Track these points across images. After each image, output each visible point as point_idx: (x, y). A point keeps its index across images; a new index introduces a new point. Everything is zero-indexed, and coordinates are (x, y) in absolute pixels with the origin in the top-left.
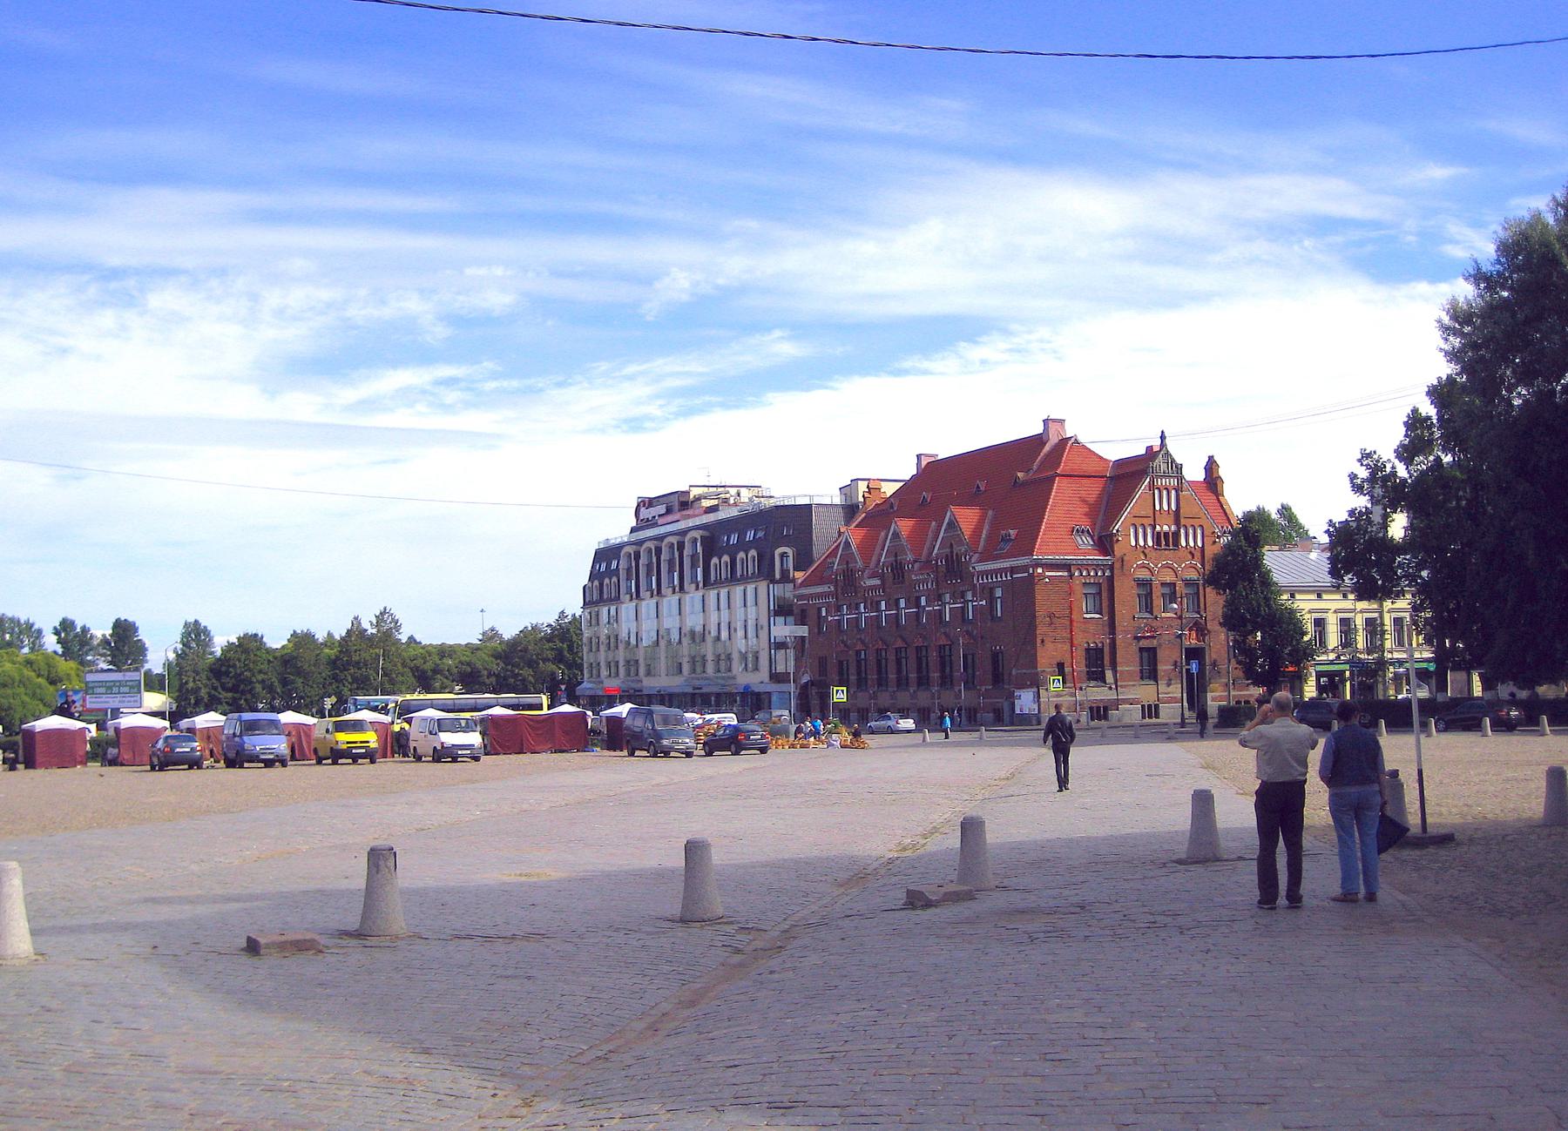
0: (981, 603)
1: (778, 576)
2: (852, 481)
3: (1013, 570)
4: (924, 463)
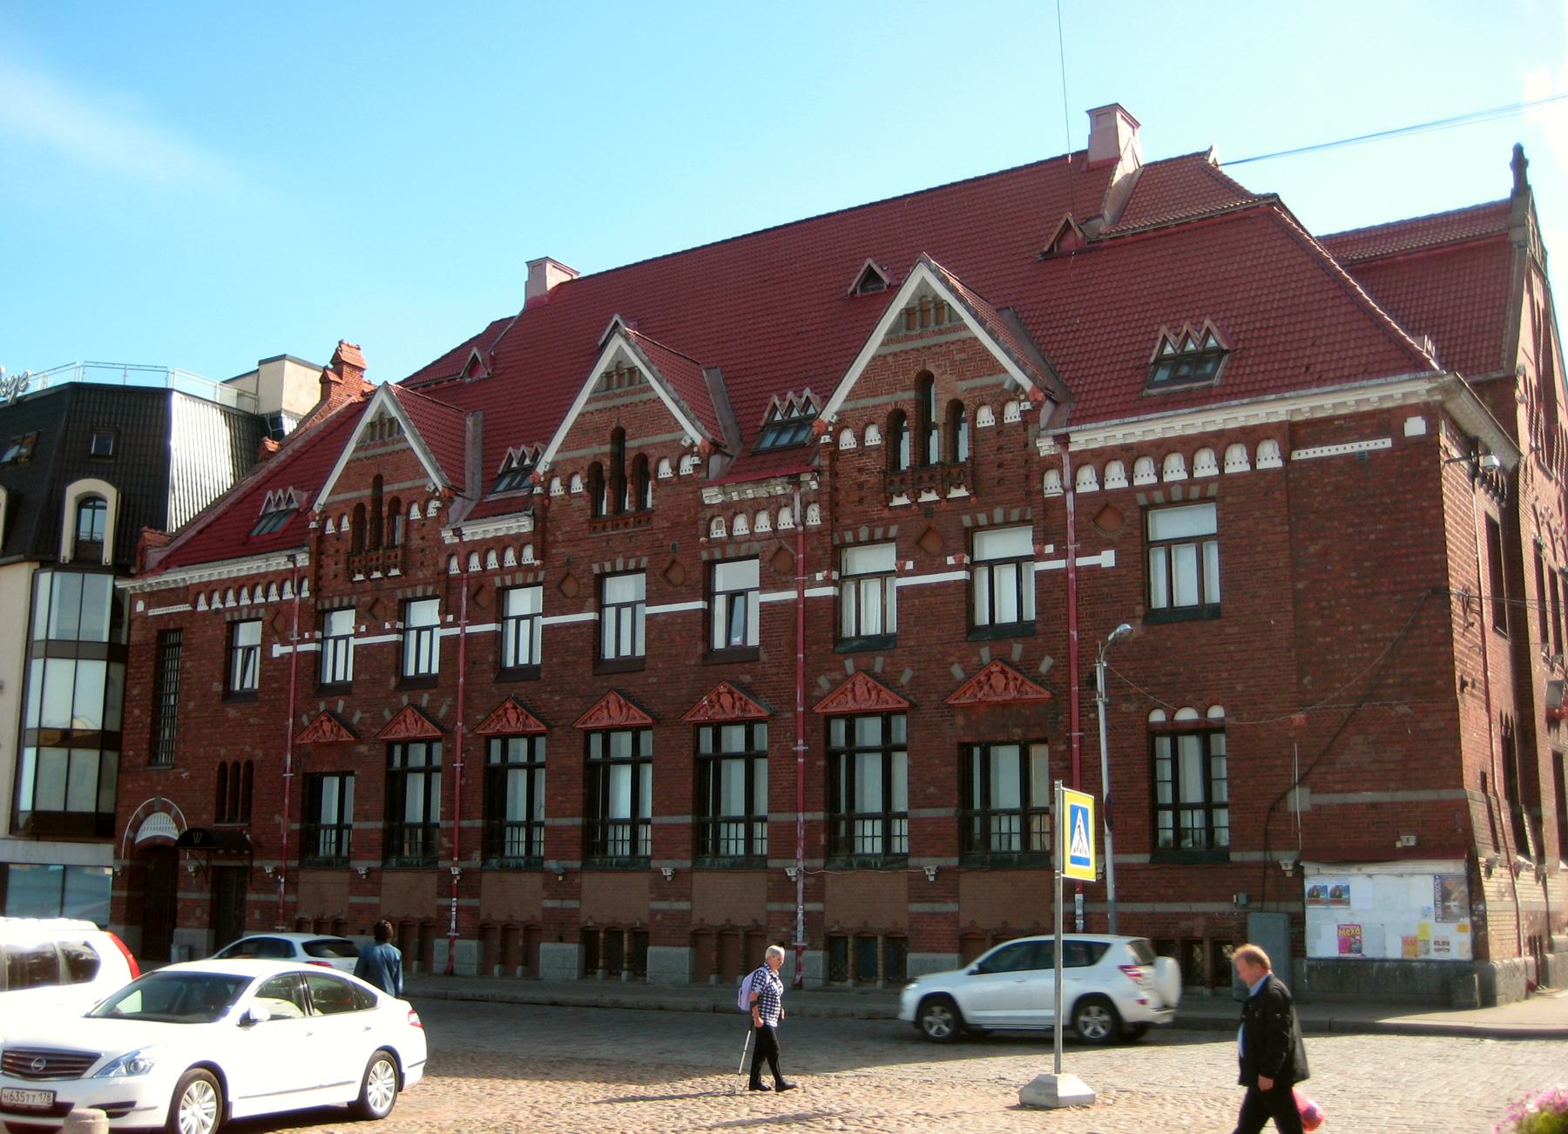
0: (1082, 562)
1: (66, 551)
2: (261, 363)
3: (1293, 434)
4: (554, 278)
